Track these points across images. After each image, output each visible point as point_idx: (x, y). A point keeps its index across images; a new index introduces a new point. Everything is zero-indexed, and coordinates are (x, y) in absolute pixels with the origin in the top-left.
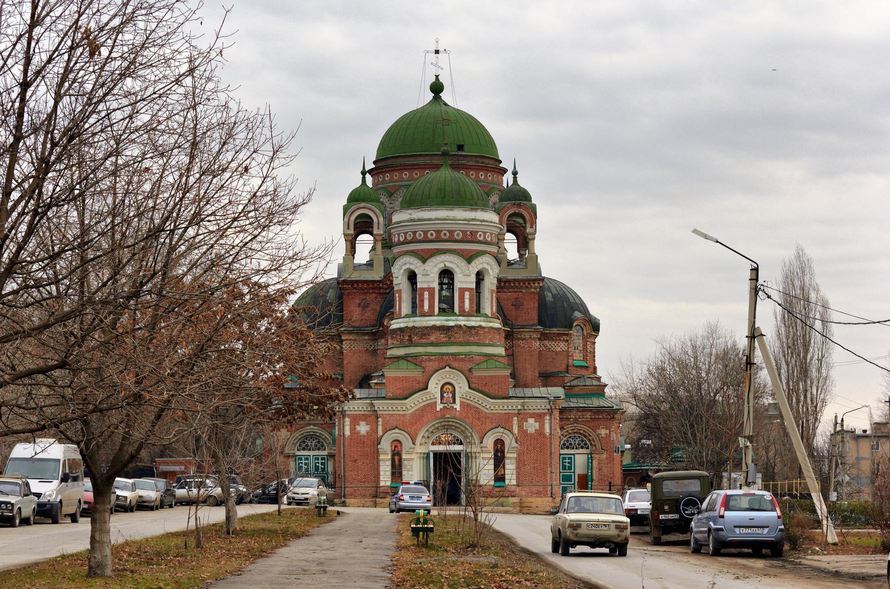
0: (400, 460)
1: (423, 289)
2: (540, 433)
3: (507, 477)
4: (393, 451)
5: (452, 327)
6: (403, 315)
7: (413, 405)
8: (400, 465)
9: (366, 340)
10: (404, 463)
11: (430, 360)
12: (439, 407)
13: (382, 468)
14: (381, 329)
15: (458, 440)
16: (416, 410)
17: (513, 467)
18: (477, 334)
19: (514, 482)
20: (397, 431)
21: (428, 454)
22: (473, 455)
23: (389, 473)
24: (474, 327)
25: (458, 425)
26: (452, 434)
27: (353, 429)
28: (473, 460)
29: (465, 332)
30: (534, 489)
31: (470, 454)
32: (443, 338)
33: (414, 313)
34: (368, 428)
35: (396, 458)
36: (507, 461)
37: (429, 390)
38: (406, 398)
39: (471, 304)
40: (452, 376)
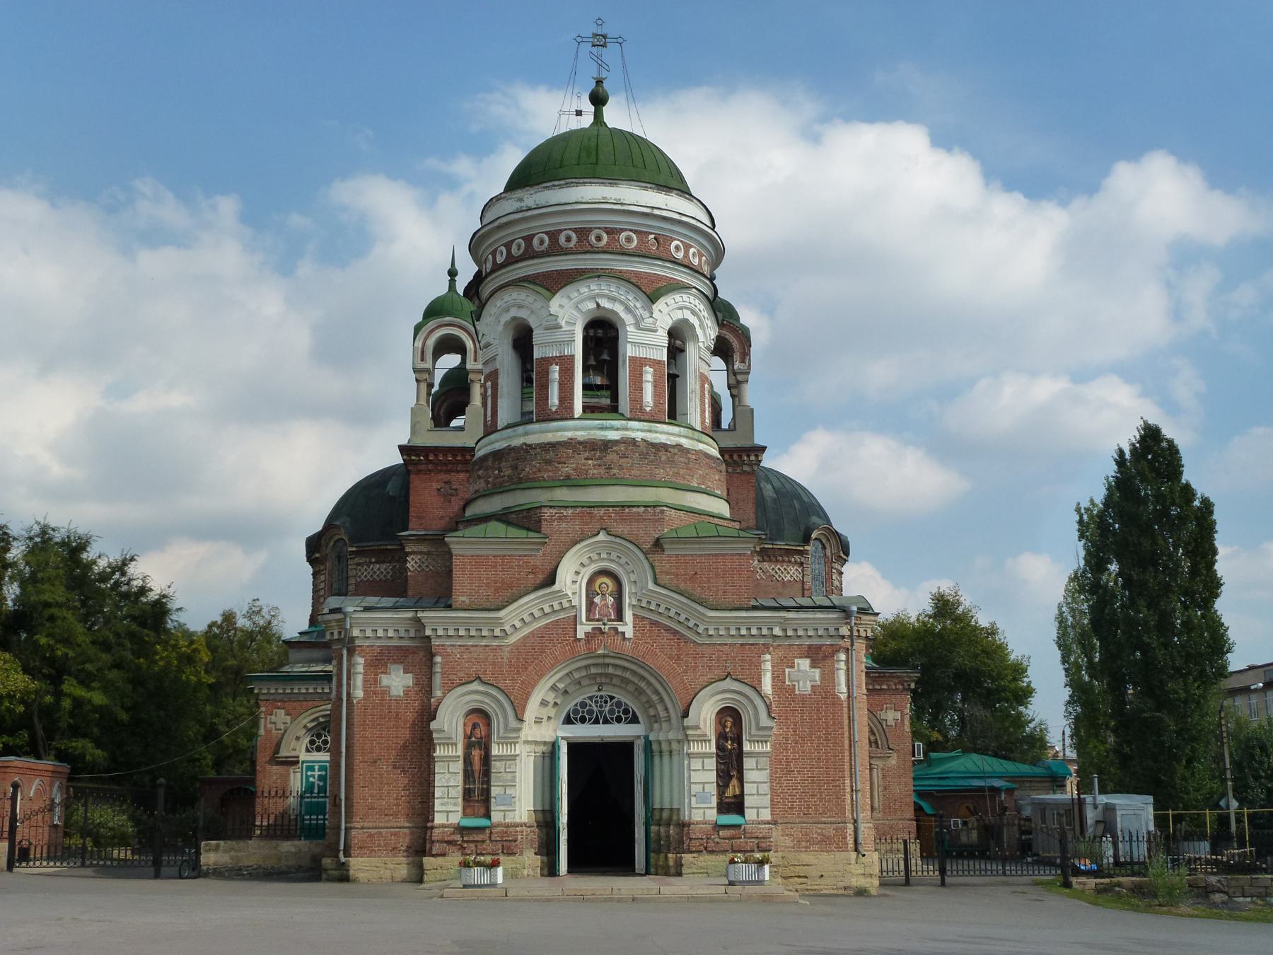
0: (487, 759)
1: (547, 361)
3: (748, 801)
4: (468, 737)
5: (616, 442)
6: (500, 425)
7: (518, 625)
8: (487, 773)
10: (496, 766)
13: (439, 780)
15: (626, 711)
16: (526, 638)
17: (763, 776)
19: (766, 815)
20: (475, 686)
21: (554, 746)
22: (665, 747)
23: (458, 792)
25: (628, 675)
26: (612, 698)
28: (666, 758)
29: (644, 456)
30: (815, 830)
31: (655, 747)
32: (592, 467)
33: (526, 418)
34: (409, 680)
35: (476, 753)
36: (748, 763)
37: (556, 587)
38: (499, 609)
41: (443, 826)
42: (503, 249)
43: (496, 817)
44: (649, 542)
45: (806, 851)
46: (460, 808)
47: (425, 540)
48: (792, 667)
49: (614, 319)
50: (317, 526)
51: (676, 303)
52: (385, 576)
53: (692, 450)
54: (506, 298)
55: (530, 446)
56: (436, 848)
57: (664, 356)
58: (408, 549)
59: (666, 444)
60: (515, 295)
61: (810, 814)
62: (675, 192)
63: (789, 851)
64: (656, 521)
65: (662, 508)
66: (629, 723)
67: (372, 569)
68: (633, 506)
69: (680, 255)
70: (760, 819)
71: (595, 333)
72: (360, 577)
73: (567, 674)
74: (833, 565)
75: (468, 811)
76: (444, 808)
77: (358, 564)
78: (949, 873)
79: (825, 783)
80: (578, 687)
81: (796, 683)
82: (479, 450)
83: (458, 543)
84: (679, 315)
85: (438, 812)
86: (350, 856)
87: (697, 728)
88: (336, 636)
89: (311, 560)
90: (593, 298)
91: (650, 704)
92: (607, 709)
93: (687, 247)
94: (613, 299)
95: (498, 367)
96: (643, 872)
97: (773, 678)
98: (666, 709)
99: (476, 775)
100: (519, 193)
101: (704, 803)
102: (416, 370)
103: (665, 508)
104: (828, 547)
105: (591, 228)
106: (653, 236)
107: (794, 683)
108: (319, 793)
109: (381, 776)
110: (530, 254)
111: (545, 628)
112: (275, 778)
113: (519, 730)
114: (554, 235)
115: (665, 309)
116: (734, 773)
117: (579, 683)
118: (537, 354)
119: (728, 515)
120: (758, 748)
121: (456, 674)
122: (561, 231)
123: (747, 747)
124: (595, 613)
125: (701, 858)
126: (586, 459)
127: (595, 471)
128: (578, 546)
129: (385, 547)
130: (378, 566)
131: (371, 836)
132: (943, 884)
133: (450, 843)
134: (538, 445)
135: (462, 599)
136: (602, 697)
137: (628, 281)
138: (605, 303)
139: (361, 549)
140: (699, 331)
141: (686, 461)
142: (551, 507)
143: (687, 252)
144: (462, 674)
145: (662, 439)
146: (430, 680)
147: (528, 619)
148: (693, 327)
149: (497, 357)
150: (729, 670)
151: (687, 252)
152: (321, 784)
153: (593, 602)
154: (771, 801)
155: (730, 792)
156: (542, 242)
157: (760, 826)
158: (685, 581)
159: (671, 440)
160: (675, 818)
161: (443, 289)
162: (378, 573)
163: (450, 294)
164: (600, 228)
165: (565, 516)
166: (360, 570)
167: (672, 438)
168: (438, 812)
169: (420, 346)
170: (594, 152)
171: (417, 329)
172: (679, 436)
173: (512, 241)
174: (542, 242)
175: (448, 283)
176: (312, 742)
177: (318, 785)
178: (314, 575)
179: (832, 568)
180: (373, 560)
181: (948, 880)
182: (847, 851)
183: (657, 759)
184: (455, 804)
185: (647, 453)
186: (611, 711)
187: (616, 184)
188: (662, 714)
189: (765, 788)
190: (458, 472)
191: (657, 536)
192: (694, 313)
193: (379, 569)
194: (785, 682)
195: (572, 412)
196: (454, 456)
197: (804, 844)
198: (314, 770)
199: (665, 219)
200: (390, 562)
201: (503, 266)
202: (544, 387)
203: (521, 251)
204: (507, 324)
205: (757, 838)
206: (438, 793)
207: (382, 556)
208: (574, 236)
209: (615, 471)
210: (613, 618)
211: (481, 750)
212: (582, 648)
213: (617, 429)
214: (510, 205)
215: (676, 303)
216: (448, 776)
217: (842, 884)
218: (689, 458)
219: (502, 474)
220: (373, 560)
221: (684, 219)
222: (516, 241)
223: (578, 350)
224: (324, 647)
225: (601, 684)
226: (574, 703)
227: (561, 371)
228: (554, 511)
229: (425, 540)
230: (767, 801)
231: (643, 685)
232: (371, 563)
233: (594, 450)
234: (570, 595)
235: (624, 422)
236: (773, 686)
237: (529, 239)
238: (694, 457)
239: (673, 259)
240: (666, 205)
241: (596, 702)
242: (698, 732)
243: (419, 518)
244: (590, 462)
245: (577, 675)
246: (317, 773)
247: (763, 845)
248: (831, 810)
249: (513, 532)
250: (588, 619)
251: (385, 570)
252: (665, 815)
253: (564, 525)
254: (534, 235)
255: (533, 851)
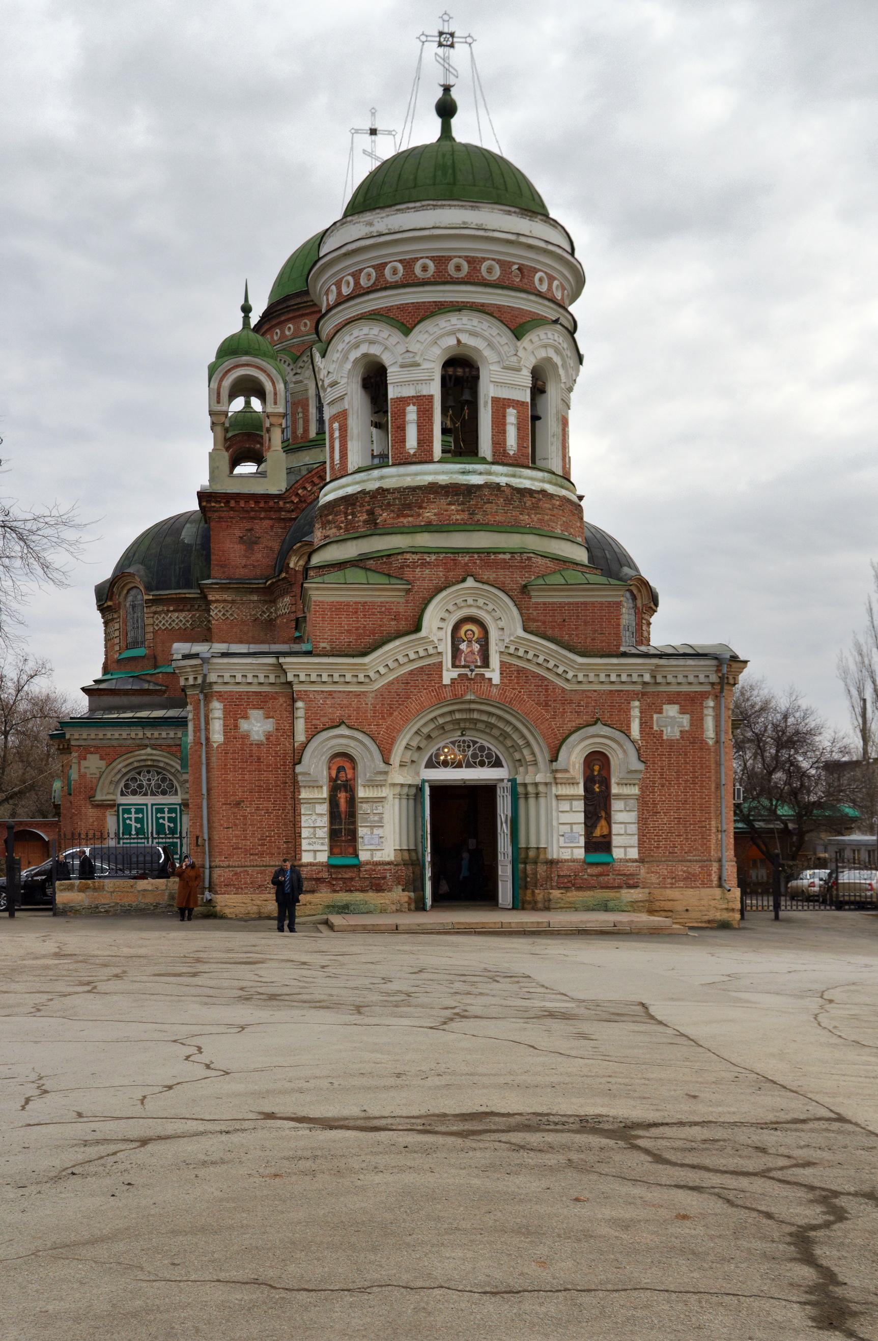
0: (352, 801)
1: (403, 401)
2: (693, 737)
3: (616, 841)
5: (479, 487)
6: (351, 468)
7: (383, 670)
8: (352, 814)
9: (254, 602)
10: (363, 809)
11: (425, 564)
12: (449, 675)
13: (305, 821)
14: (284, 575)
15: (489, 756)
16: (391, 683)
17: (632, 817)
18: (535, 507)
19: (634, 853)
21: (420, 789)
22: (531, 789)
23: (323, 833)
24: (530, 492)
25: (493, 720)
26: (475, 743)
27: (231, 728)
28: (532, 801)
29: (508, 501)
30: (680, 869)
31: (520, 790)
32: (455, 512)
33: (381, 460)
34: (269, 725)
35: (342, 796)
36: (616, 805)
37: (423, 633)
38: (364, 654)
39: (520, 438)
40: (481, 602)
41: (311, 864)
42: (350, 279)
43: (364, 856)
44: (515, 590)
45: (672, 887)
46: (326, 848)
47: (229, 588)
48: (660, 712)
49: (475, 356)
50: (106, 573)
51: (540, 340)
52: (184, 624)
53: (556, 495)
54: (356, 333)
55: (387, 490)
56: (306, 885)
57: (527, 398)
58: (210, 598)
59: (530, 490)
60: (366, 330)
61: (676, 853)
62: (540, 217)
63: (655, 888)
64: (523, 568)
65: (529, 555)
66: (492, 766)
67: (171, 617)
68: (499, 553)
69: (544, 288)
70: (628, 857)
71: (455, 372)
72: (157, 625)
73: (432, 720)
74: (644, 615)
75: (336, 850)
76: (311, 848)
77: (155, 613)
78: (783, 908)
79: (691, 824)
80: (441, 731)
81: (664, 729)
82: (325, 495)
83: (317, 589)
84: (542, 354)
85: (305, 851)
86: (216, 893)
87: (566, 771)
88: (191, 682)
89: (102, 609)
90: (452, 333)
91: (515, 747)
92: (470, 753)
93: (551, 279)
94: (473, 334)
95: (347, 407)
96: (511, 907)
97: (641, 724)
98: (533, 754)
99: (343, 816)
100: (368, 217)
101: (572, 842)
102: (211, 413)
103: (532, 555)
104: (639, 597)
105: (449, 257)
106: (516, 267)
107: (662, 729)
108: (137, 834)
109: (245, 817)
110: (381, 286)
111: (409, 674)
112: (91, 820)
113: (386, 773)
114: (408, 264)
115: (530, 347)
116: (603, 814)
117: (443, 728)
118: (392, 393)
119: (586, 562)
120: (626, 790)
121: (319, 719)
122: (417, 259)
123: (615, 790)
124: (460, 660)
125: (569, 894)
126: (449, 504)
127: (458, 517)
128: (444, 593)
129: (184, 596)
130: (176, 614)
131: (236, 874)
132: (777, 918)
133: (318, 880)
134: (395, 489)
135: (322, 645)
136: (464, 742)
137: (491, 315)
138: (465, 339)
139: (158, 597)
140: (561, 371)
141: (551, 507)
142: (413, 553)
143: (550, 285)
144: (324, 719)
145: (527, 484)
146: (293, 724)
147: (392, 665)
148: (555, 366)
149: (346, 398)
150: (597, 716)
151: (550, 285)
152: (139, 826)
153: (459, 649)
154: (639, 841)
155: (597, 832)
156: (395, 272)
157: (628, 864)
158: (553, 628)
159: (536, 486)
160: (542, 856)
161: (236, 326)
162: (177, 621)
163: (245, 332)
164: (460, 257)
165: (429, 563)
166: (157, 619)
167: (537, 483)
168: (305, 851)
169: (216, 387)
170: (450, 171)
171: (212, 369)
172: (543, 481)
173: (361, 270)
174: (395, 272)
175: (241, 320)
176: (127, 786)
177: (136, 826)
178: (106, 623)
179: (643, 618)
180: (171, 608)
181: (781, 914)
182: (712, 887)
183: (522, 802)
184: (322, 844)
185: (512, 498)
186: (474, 756)
187: (477, 207)
188: (529, 758)
189: (633, 829)
190: (261, 519)
191: (524, 583)
192: (558, 351)
193: (178, 618)
194: (653, 728)
195: (432, 455)
196: (257, 502)
197: (669, 881)
198: (130, 813)
199: (530, 247)
200: (188, 611)
201: (350, 298)
202: (401, 429)
203: (372, 282)
204: (356, 361)
205: (625, 875)
206: (305, 833)
207: (181, 604)
208: (431, 264)
209: (478, 517)
210: (479, 664)
211: (346, 792)
212: (447, 693)
213: (481, 474)
214: (357, 230)
215: (540, 340)
216: (314, 817)
217: (706, 918)
218: (554, 505)
219: (356, 519)
220: (171, 608)
221: (550, 247)
222: (365, 271)
223: (435, 389)
224: (124, 695)
225: (464, 730)
226: (437, 747)
227: (419, 411)
228: (416, 557)
229: (229, 588)
230: (634, 840)
231: (508, 729)
232: (168, 611)
233: (456, 495)
234: (436, 641)
235: (487, 466)
236: (641, 732)
237: (380, 268)
238: (558, 503)
239: (536, 292)
240: (531, 232)
241: (459, 746)
242: (567, 775)
243: (221, 567)
244: (453, 507)
245: (441, 721)
246: (166, 815)
247: (631, 882)
248: (696, 849)
249: (375, 578)
250: (454, 666)
251: (184, 618)
252: (532, 854)
253: (427, 571)
254: (386, 264)
255: (400, 887)
